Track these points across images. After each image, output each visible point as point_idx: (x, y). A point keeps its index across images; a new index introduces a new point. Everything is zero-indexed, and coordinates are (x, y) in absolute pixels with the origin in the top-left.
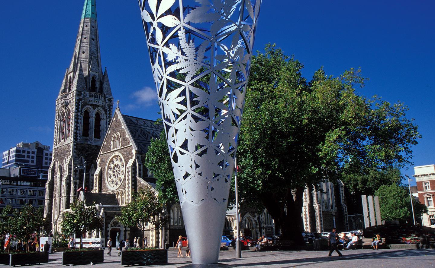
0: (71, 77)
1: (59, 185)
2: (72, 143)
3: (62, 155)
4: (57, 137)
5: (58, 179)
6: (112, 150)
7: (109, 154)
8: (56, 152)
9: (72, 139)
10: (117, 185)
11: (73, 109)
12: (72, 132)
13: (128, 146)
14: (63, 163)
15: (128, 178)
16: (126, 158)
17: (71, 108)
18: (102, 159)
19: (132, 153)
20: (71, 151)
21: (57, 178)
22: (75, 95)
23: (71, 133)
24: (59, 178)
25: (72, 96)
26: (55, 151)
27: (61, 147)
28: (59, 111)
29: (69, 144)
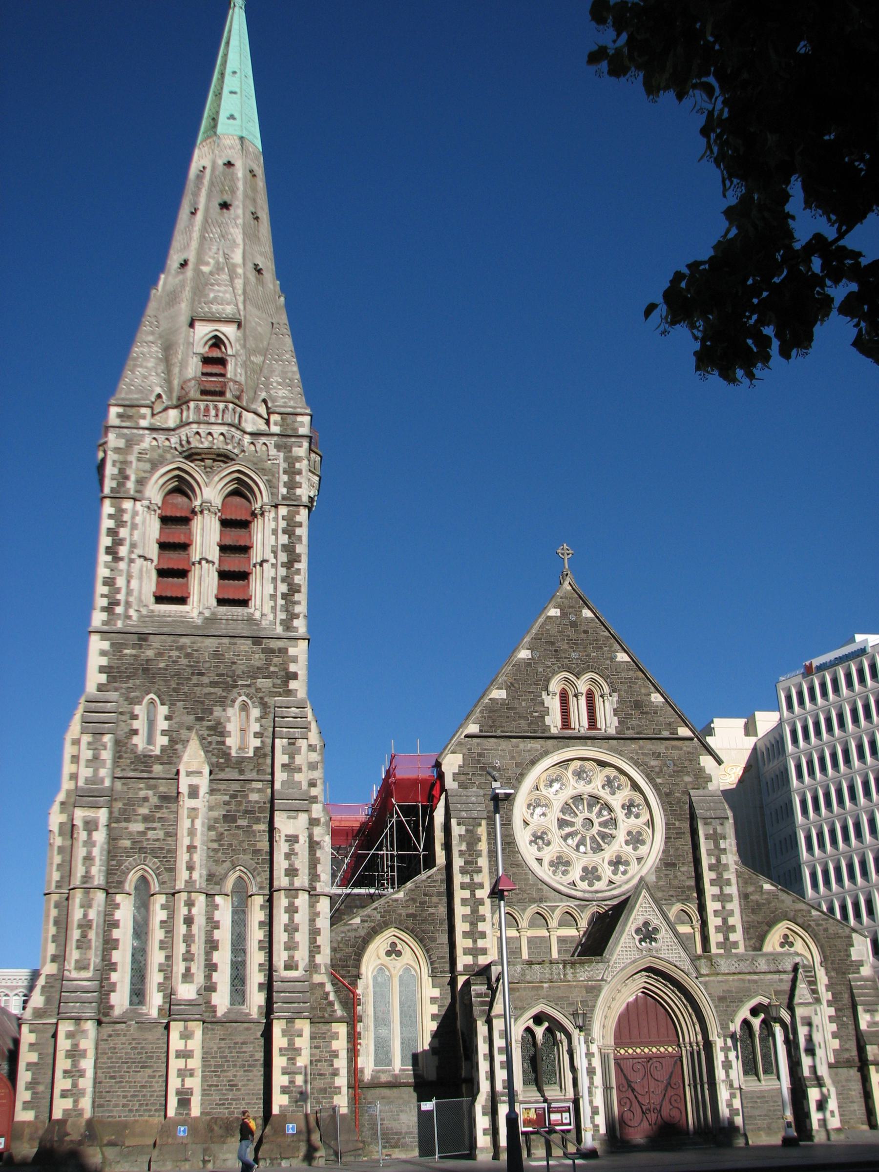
0: (217, 342)
1: (203, 824)
2: (303, 645)
3: (205, 680)
4: (128, 582)
5: (194, 792)
6: (554, 731)
7: (536, 745)
8: (127, 651)
9: (300, 625)
10: (598, 885)
11: (292, 485)
12: (294, 589)
13: (666, 734)
14: (219, 723)
15: (714, 861)
16: (659, 781)
17: (272, 486)
18: (480, 755)
19: (702, 770)
20: (295, 676)
21: (184, 789)
22: (304, 430)
23: (284, 596)
24: (204, 789)
25: (275, 429)
26: (117, 647)
27: (184, 640)
28: (139, 460)
29: (275, 644)
